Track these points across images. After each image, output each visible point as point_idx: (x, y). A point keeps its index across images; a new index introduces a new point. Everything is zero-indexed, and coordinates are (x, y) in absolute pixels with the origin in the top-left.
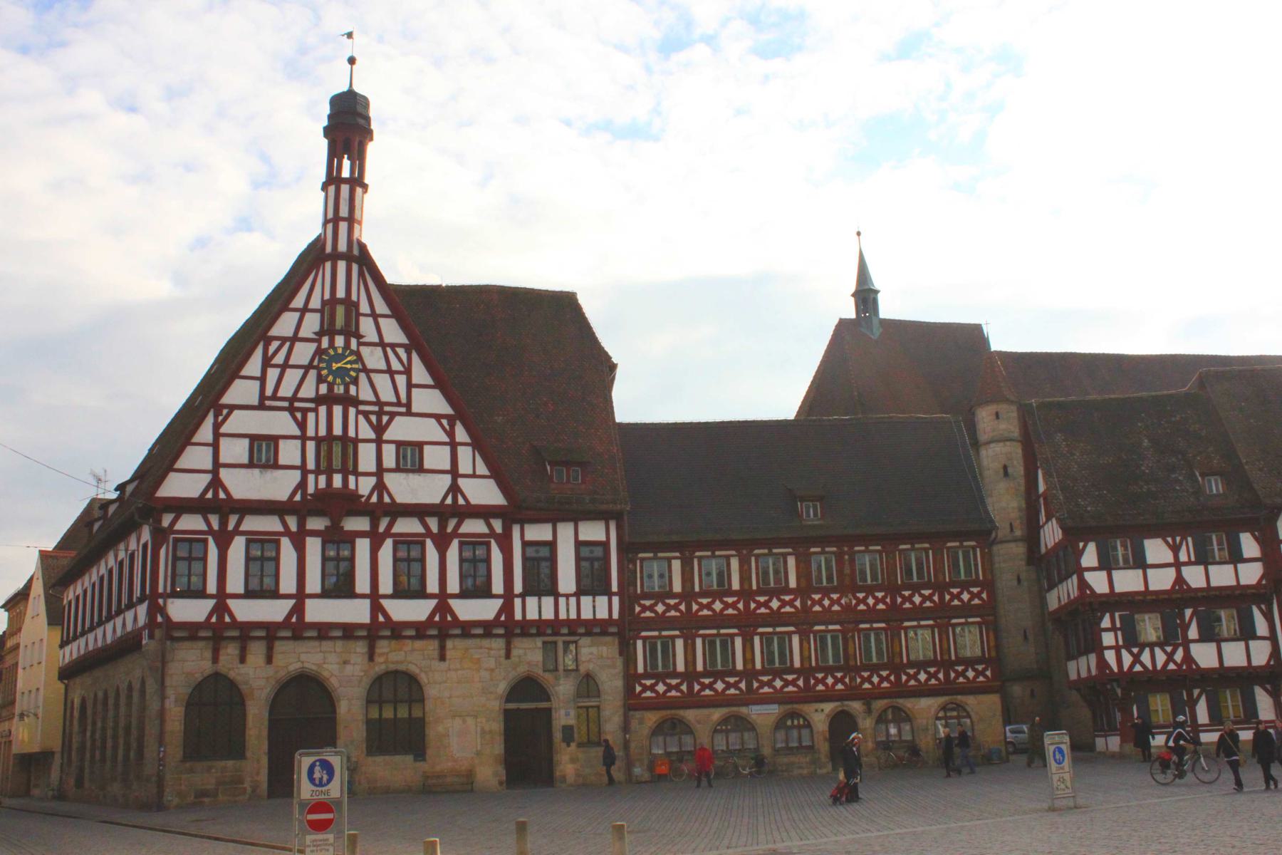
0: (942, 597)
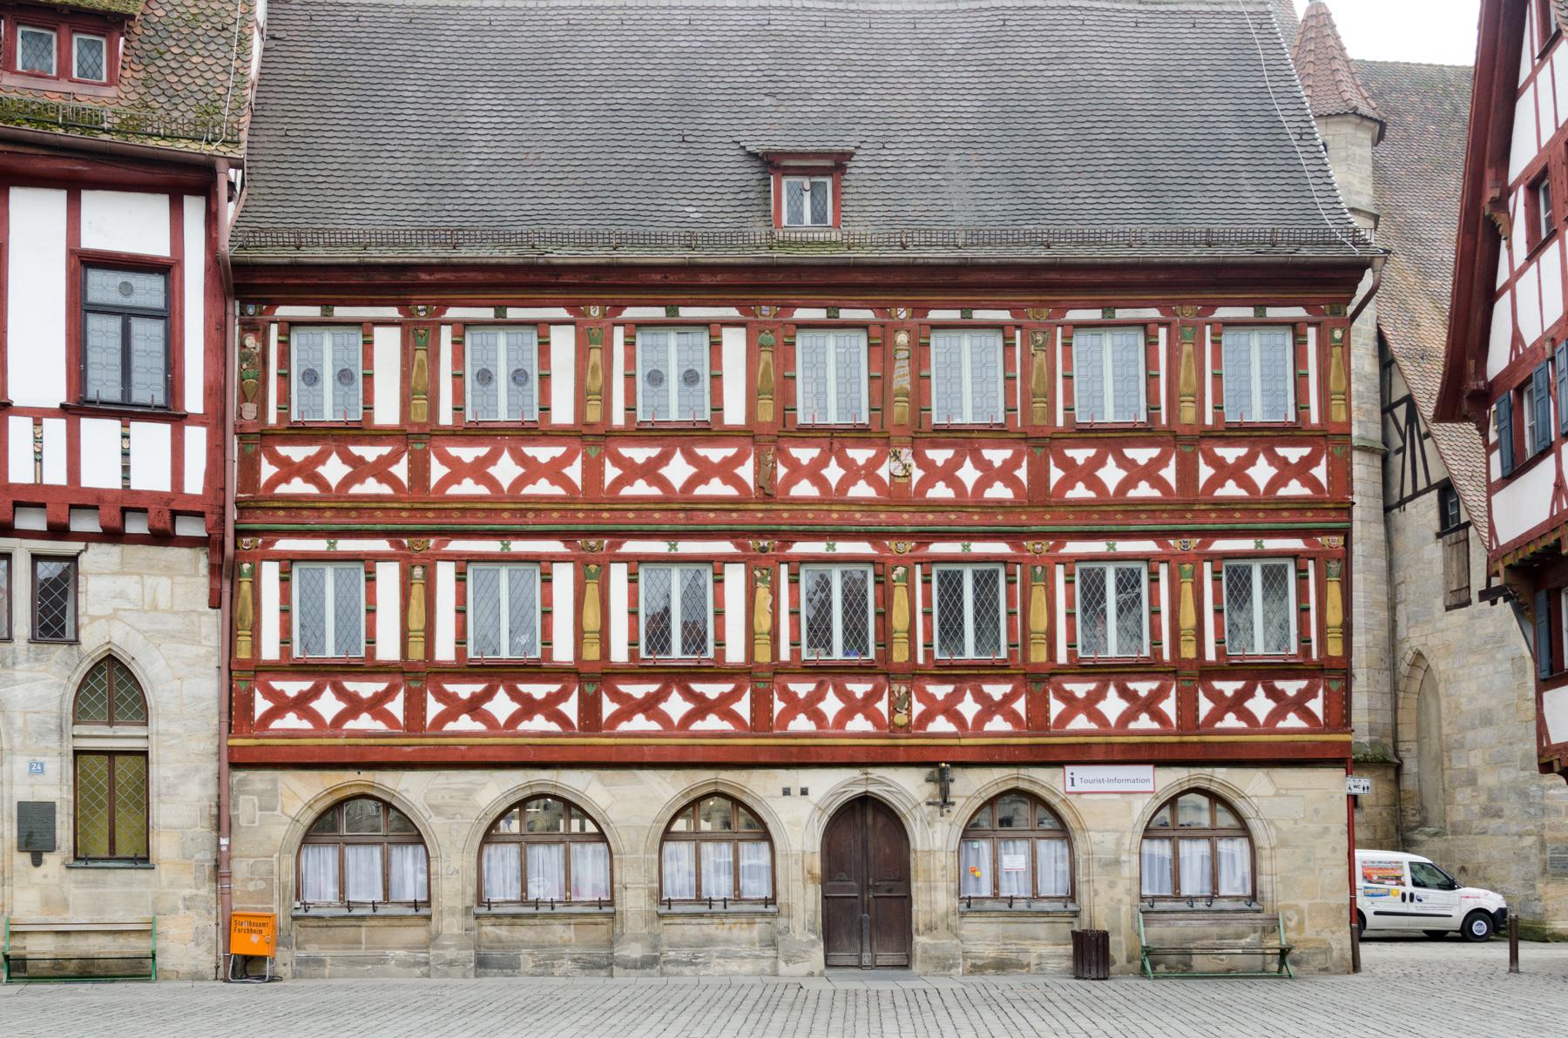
0: (1187, 472)
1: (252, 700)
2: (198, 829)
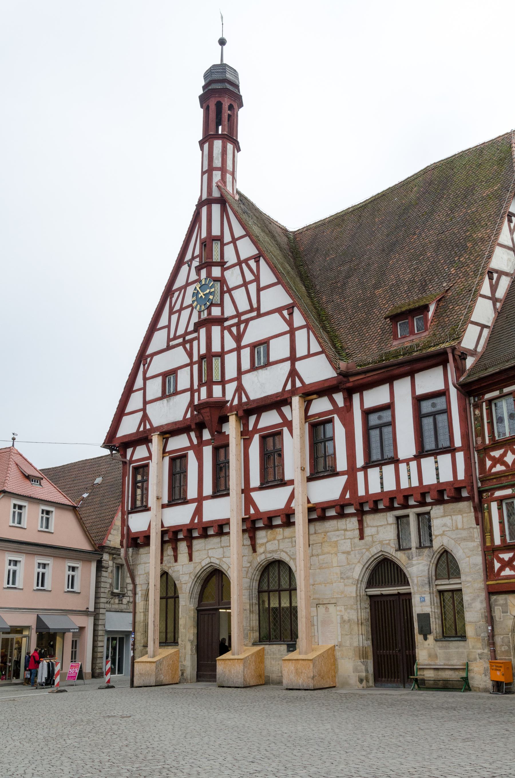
1: (493, 563)
2: (481, 623)
